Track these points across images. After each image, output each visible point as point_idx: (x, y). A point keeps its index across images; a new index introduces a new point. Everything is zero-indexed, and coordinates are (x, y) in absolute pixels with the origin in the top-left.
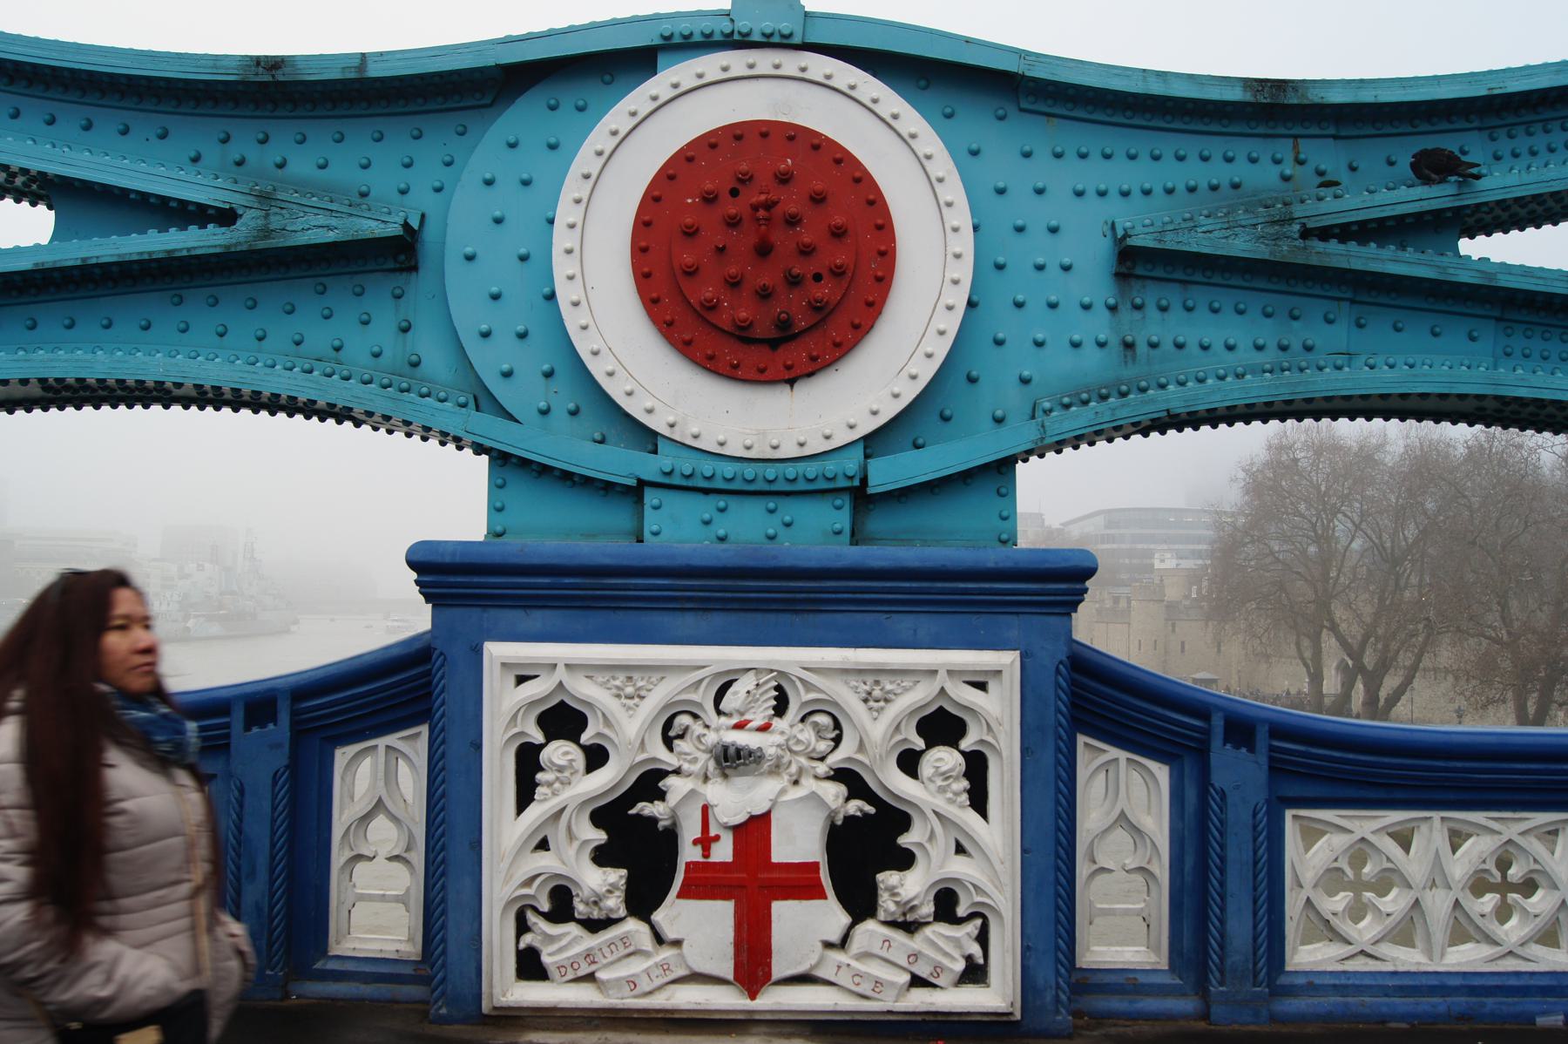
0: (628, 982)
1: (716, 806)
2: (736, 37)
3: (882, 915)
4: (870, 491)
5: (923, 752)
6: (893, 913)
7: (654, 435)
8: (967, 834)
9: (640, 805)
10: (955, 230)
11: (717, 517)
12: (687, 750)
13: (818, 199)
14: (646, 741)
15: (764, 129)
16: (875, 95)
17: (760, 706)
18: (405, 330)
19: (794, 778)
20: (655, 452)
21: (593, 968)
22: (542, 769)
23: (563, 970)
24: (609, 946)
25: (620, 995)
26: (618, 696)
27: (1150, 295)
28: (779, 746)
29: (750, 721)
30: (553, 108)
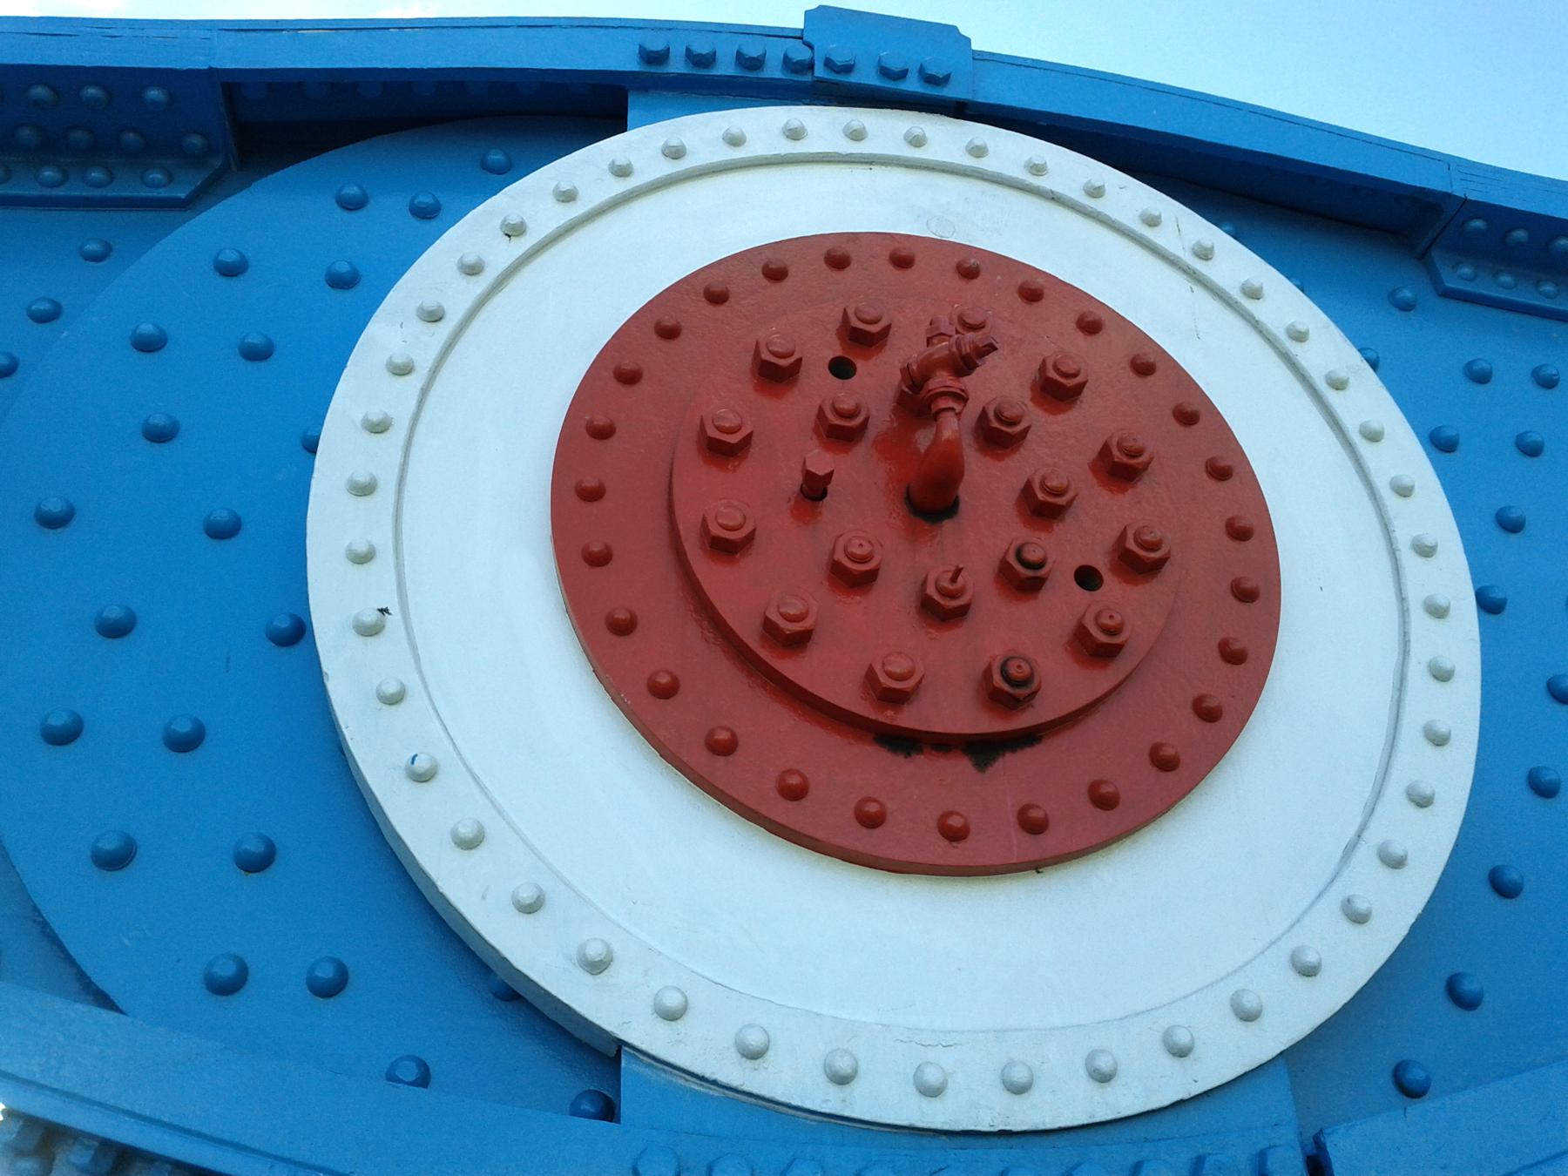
20: (609, 1111)
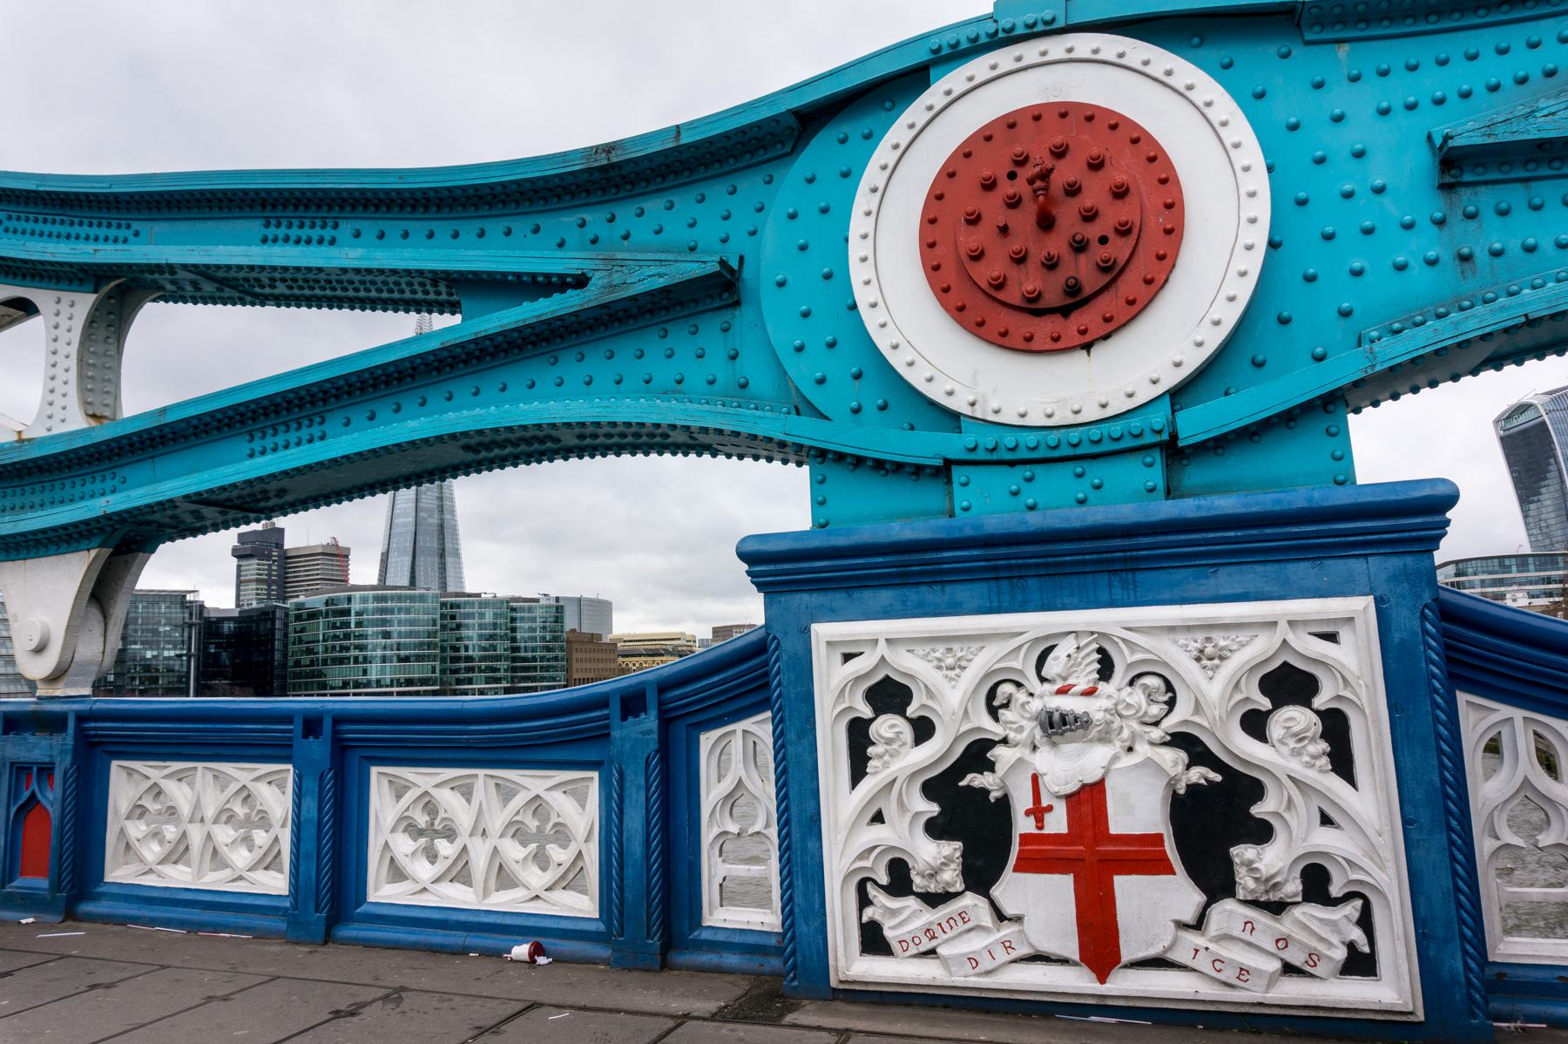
0: (969, 959)
1: (1045, 774)
2: (1001, 35)
3: (1241, 894)
4: (1181, 444)
5: (1269, 712)
6: (1252, 891)
7: (955, 416)
8: (1336, 805)
9: (970, 777)
10: (1246, 169)
11: (1025, 487)
12: (1013, 719)
13: (1096, 165)
14: (970, 710)
15: (1036, 113)
16: (1145, 58)
17: (1083, 670)
18: (733, 358)
19: (1128, 744)
21: (934, 943)
22: (874, 744)
23: (904, 944)
24: (948, 922)
25: (963, 973)
26: (939, 668)
27: (1485, 200)
28: (1106, 710)
29: (1073, 686)
30: (843, 141)
